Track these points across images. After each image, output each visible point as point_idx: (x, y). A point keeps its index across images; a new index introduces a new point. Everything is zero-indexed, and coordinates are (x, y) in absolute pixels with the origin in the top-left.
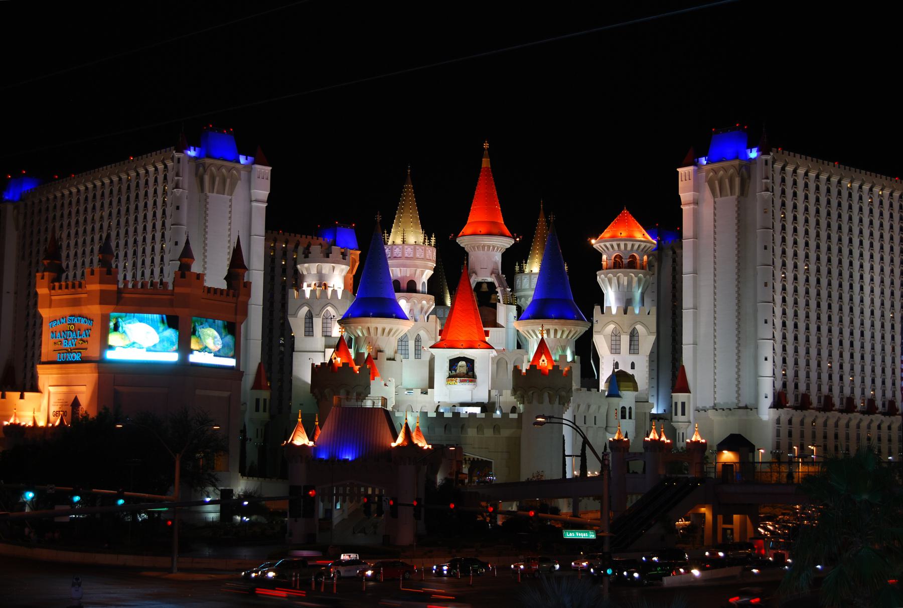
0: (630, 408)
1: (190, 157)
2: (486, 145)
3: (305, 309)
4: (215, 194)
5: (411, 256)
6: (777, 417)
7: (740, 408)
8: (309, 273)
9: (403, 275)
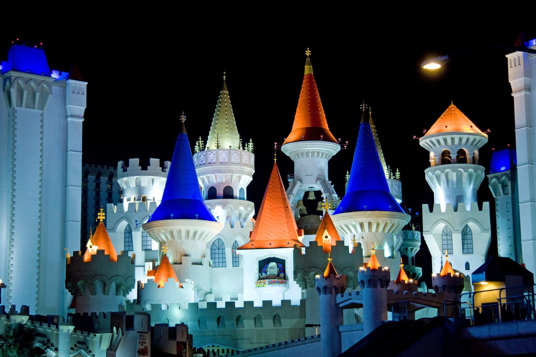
2: (308, 53)
3: (124, 224)
4: (23, 108)
5: (226, 160)
8: (128, 187)
9: (219, 180)
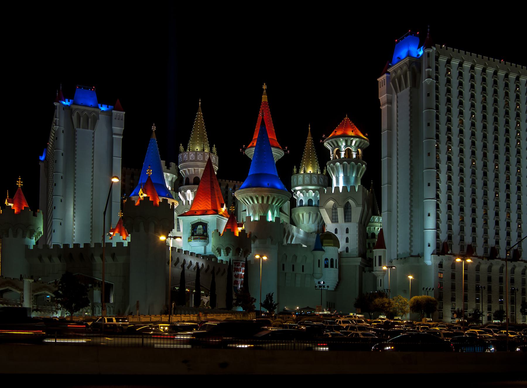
0: (332, 260)
1: (65, 105)
6: (438, 262)
7: (412, 256)
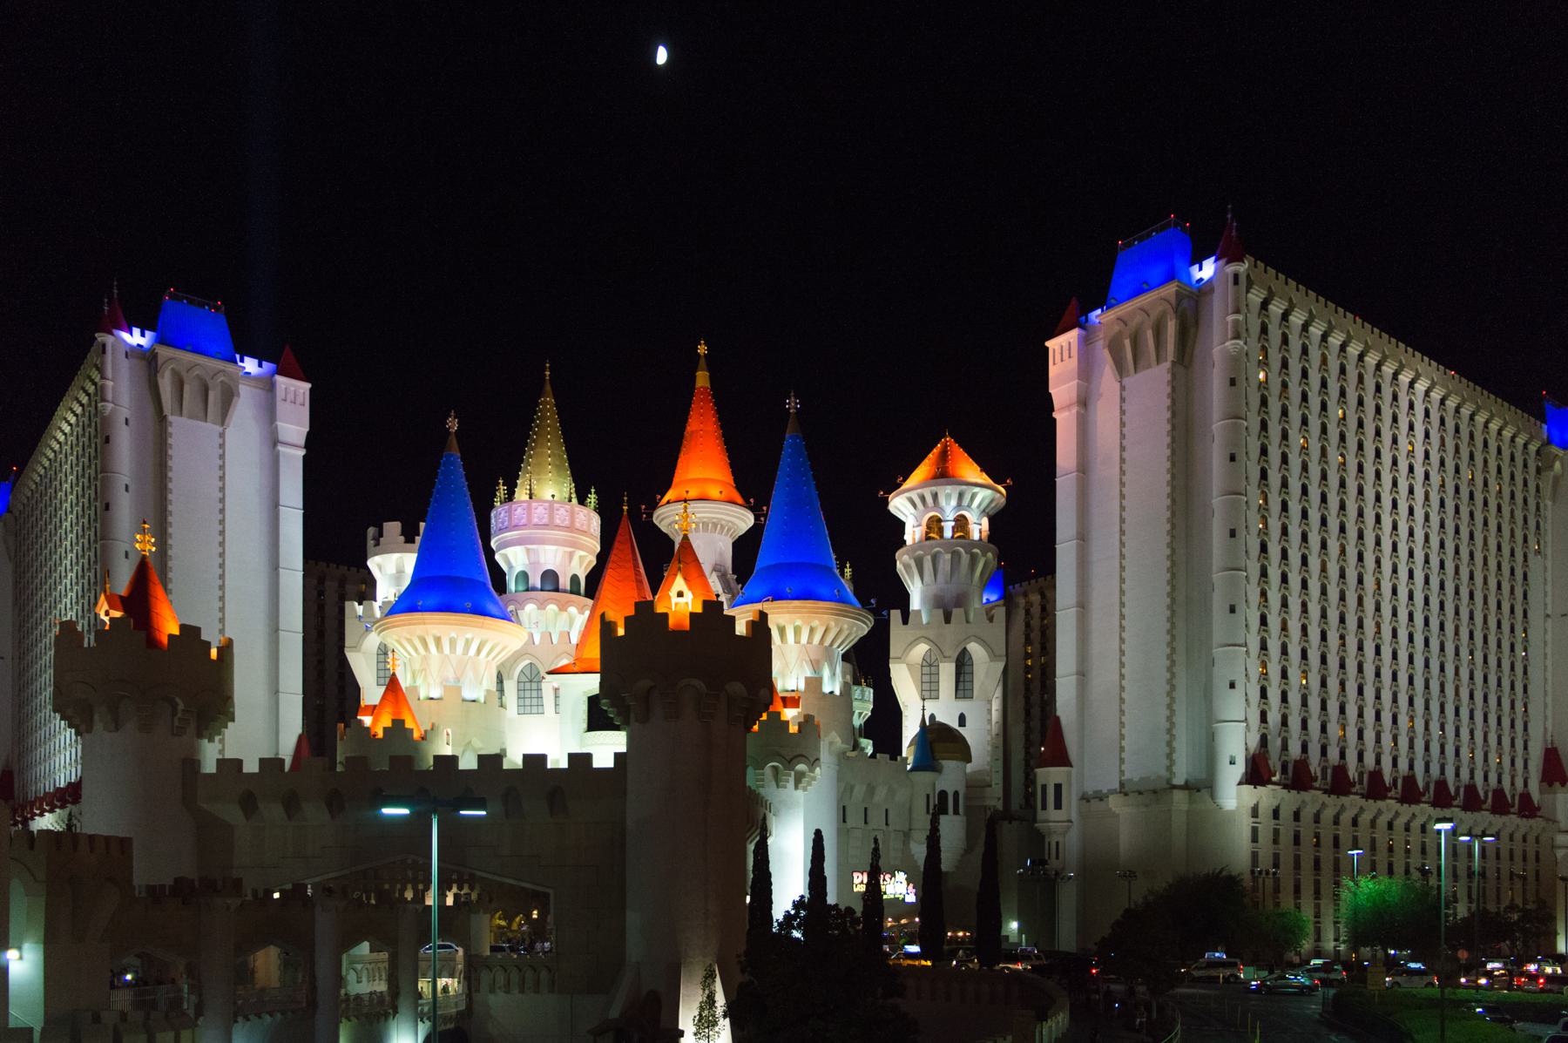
4: (184, 420)
5: (545, 521)
